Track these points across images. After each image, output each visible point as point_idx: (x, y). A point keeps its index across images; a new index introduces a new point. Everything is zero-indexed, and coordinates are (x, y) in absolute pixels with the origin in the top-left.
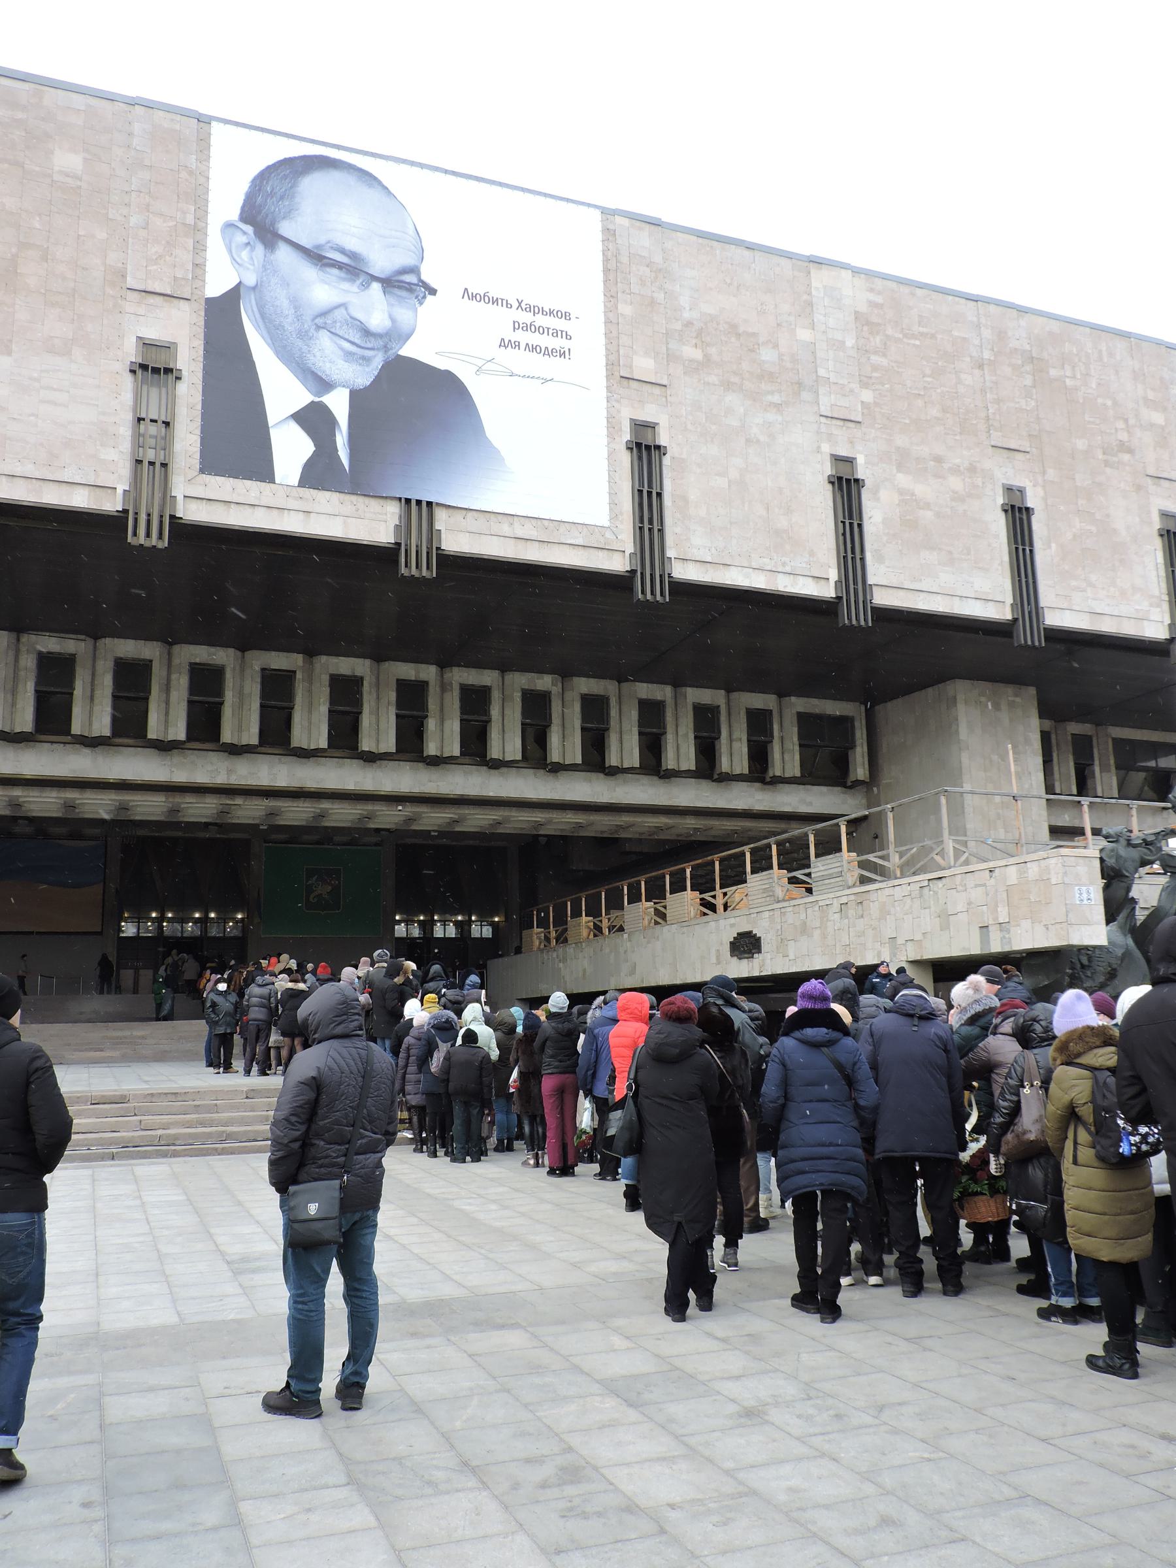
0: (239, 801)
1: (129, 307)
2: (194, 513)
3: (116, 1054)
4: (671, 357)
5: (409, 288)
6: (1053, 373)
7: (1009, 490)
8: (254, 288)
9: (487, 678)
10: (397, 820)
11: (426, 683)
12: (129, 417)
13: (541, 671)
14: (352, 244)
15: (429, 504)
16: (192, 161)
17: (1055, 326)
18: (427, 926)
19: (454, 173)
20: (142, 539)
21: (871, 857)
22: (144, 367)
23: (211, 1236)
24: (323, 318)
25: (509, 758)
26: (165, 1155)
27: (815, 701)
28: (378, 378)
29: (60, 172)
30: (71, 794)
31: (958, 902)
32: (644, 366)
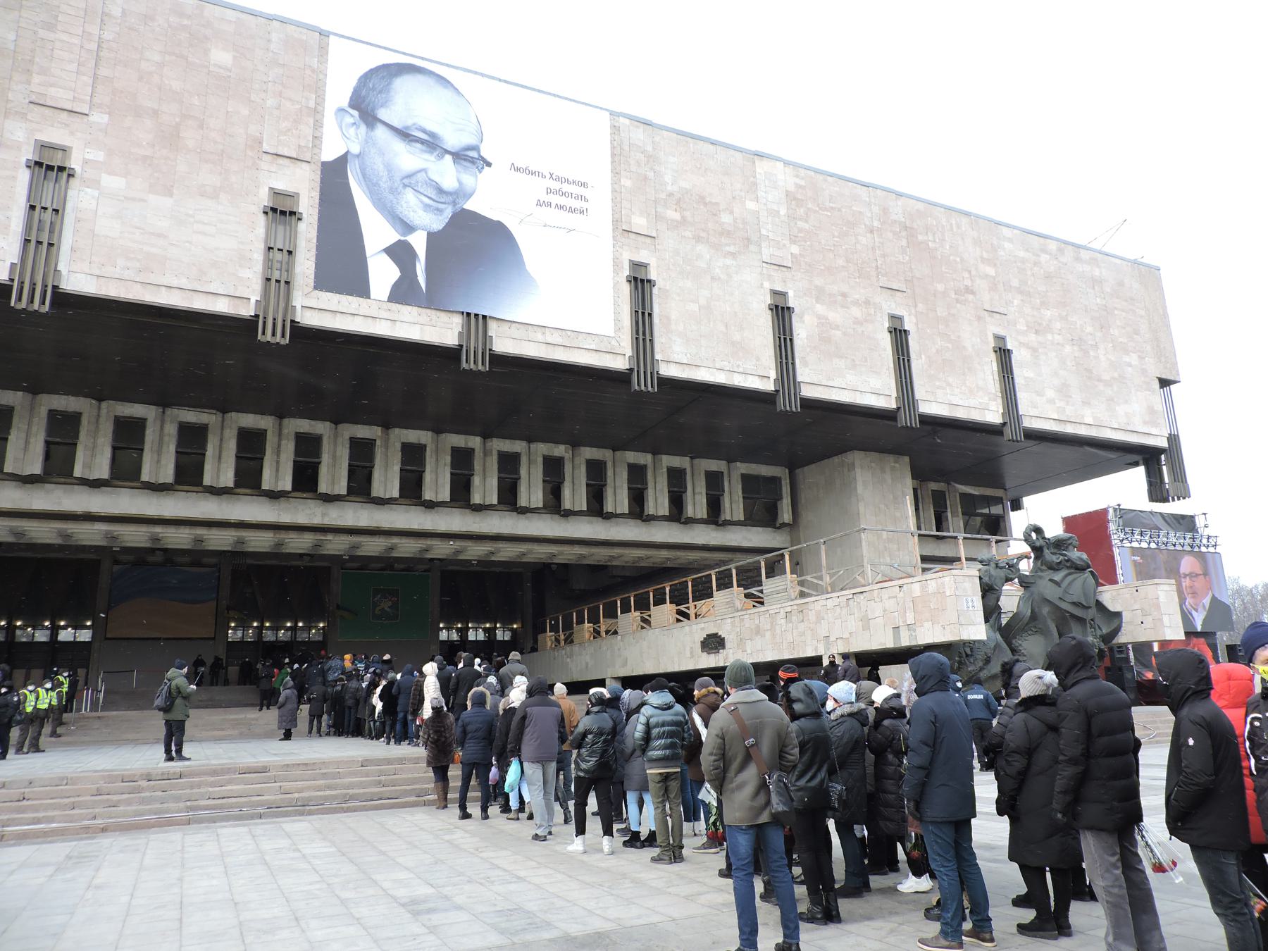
0: (330, 537)
1: (264, 166)
2: (309, 319)
3: (235, 732)
4: (658, 217)
5: (472, 161)
6: (920, 238)
7: (893, 317)
8: (358, 156)
9: (517, 446)
10: (448, 551)
11: (473, 450)
12: (261, 246)
13: (557, 442)
14: (430, 127)
15: (484, 317)
16: (314, 63)
18: (463, 632)
19: (505, 82)
20: (269, 337)
21: (808, 578)
22: (274, 210)
23: (375, 882)
24: (409, 180)
25: (533, 506)
26: (302, 814)
27: (754, 466)
28: (448, 225)
29: (215, 65)
31: (876, 610)
32: (639, 222)
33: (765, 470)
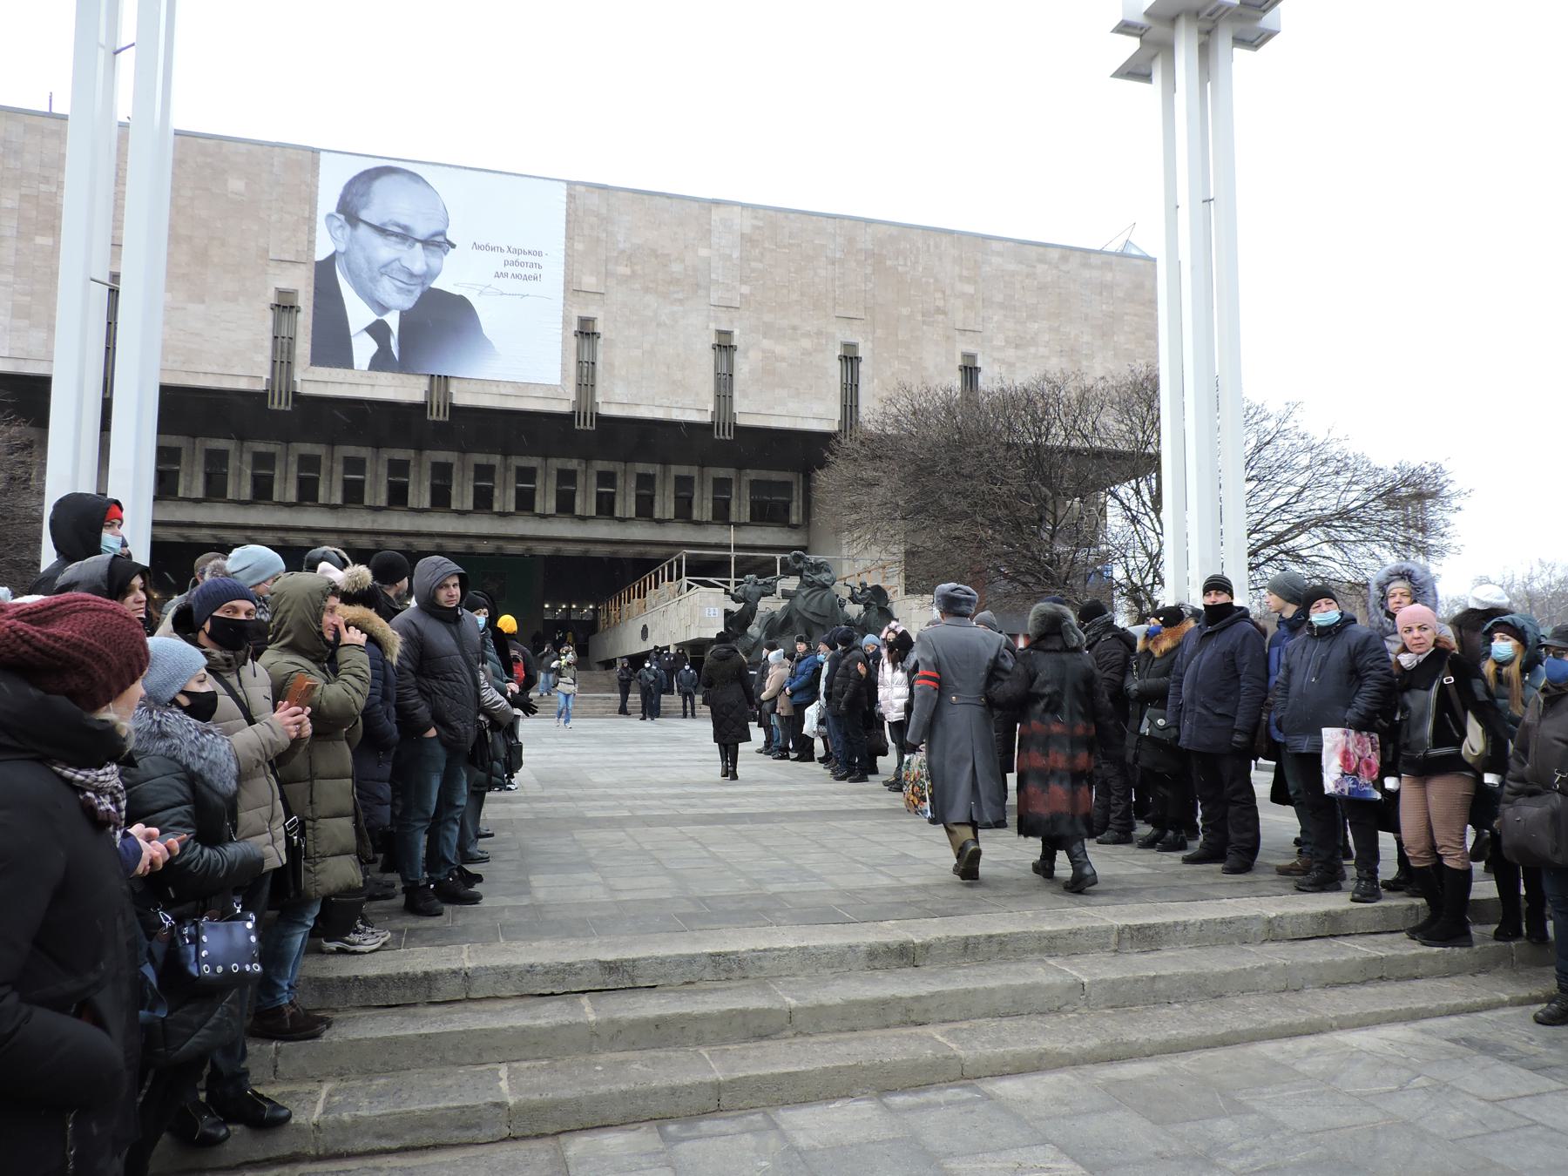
4: (608, 274)
5: (439, 245)
6: (889, 263)
12: (270, 336)
13: (570, 457)
14: (404, 221)
17: (894, 230)
24: (385, 269)
30: (281, 535)
32: (589, 282)
33: (775, 476)
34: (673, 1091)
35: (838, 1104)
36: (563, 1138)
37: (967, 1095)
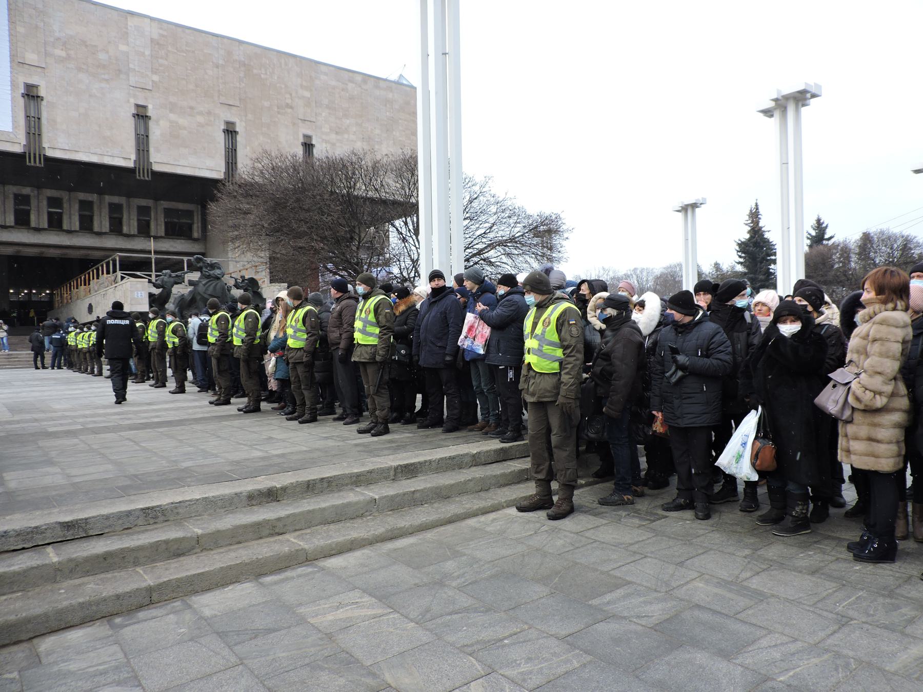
6: (255, 71)
25: (8, 224)
27: (174, 203)
34: (118, 597)
35: (230, 587)
36: (35, 641)
37: (310, 570)
